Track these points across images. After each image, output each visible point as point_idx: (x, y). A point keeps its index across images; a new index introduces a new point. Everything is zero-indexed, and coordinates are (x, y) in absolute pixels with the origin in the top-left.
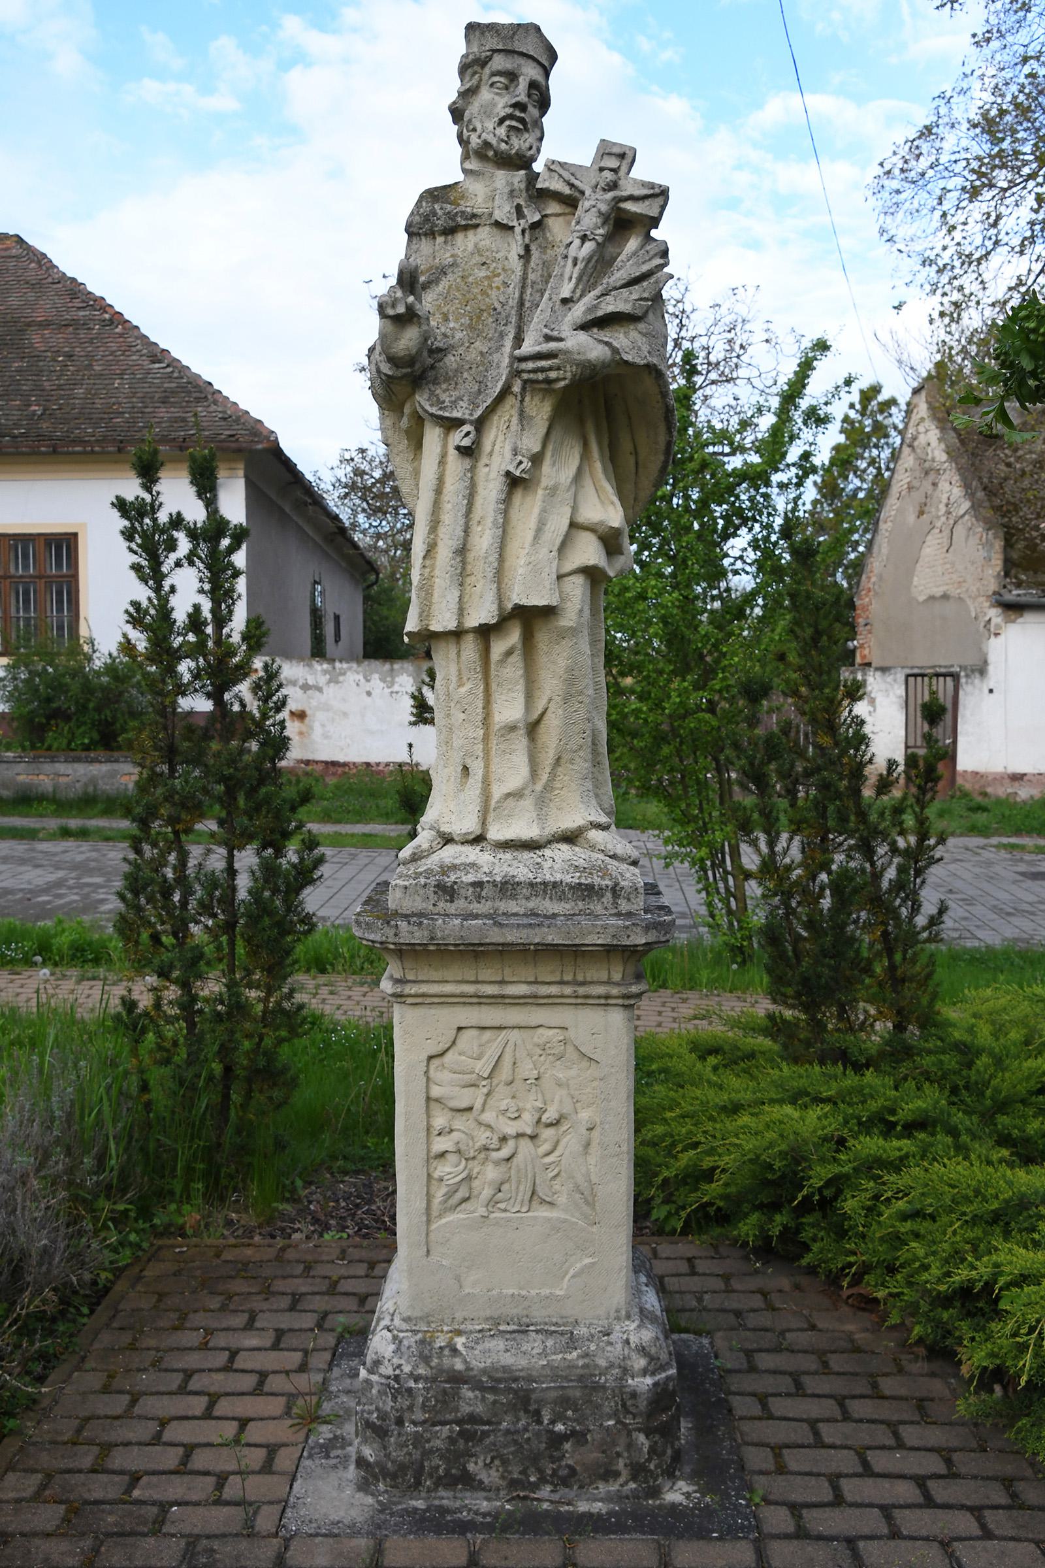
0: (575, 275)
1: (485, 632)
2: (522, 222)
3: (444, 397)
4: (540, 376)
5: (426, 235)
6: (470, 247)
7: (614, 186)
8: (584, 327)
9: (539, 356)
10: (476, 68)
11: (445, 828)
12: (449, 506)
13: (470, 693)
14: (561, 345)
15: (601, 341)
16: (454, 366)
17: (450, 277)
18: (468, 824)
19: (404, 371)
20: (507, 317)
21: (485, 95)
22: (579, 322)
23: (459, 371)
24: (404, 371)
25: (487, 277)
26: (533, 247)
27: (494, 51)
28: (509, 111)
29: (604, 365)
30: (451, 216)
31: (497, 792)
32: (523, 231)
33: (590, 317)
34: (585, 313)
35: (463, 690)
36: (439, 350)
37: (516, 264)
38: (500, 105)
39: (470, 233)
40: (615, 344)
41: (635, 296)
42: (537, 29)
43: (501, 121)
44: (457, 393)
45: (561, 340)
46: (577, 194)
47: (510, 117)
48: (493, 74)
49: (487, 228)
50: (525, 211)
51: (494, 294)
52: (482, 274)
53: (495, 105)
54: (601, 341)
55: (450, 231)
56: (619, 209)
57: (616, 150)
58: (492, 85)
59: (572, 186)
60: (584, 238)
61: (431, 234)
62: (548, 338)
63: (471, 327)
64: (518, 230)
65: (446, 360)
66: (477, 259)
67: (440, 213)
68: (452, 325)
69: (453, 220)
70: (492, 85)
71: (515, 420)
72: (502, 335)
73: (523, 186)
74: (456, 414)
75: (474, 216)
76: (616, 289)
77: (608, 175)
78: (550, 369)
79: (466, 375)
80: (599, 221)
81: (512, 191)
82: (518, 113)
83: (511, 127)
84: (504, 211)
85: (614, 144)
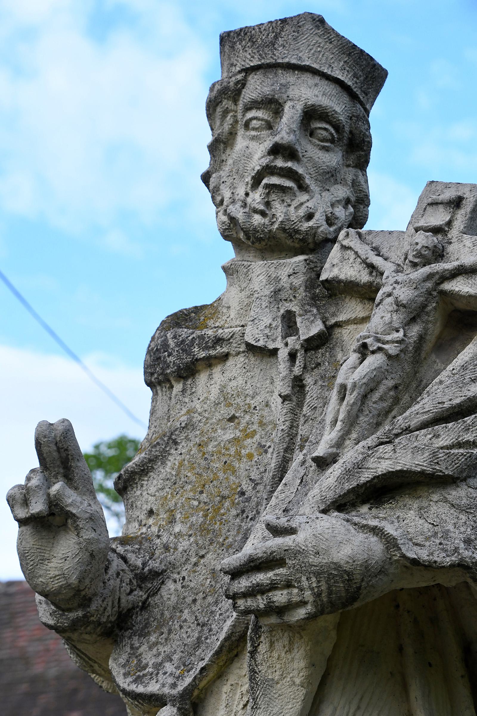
2: (291, 340)
4: (261, 602)
7: (438, 254)
8: (342, 504)
9: (254, 565)
10: (227, 104)
15: (364, 528)
16: (174, 599)
17: (183, 447)
19: (72, 615)
21: (241, 142)
22: (331, 496)
23: (177, 608)
24: (72, 615)
25: (236, 440)
26: (309, 380)
27: (248, 71)
28: (265, 161)
29: (370, 571)
30: (185, 346)
32: (292, 356)
33: (348, 486)
34: (340, 480)
36: (156, 574)
37: (278, 411)
38: (257, 156)
39: (217, 370)
40: (390, 529)
41: (444, 440)
42: (319, 22)
43: (257, 181)
44: (167, 649)
45: (292, 531)
47: (268, 170)
48: (247, 109)
49: (241, 359)
50: (299, 320)
51: (242, 466)
52: (229, 435)
54: (364, 528)
56: (443, 293)
57: (448, 195)
59: (371, 267)
60: (364, 350)
62: (276, 531)
63: (203, 529)
64: (283, 354)
65: (164, 592)
66: (225, 412)
67: (172, 343)
68: (177, 529)
73: (299, 281)
74: (153, 688)
75: (219, 341)
76: (408, 430)
77: (431, 240)
78: (273, 587)
79: (186, 614)
80: (397, 319)
81: (277, 292)
82: (280, 163)
83: (270, 187)
84: (261, 327)
85: (447, 186)
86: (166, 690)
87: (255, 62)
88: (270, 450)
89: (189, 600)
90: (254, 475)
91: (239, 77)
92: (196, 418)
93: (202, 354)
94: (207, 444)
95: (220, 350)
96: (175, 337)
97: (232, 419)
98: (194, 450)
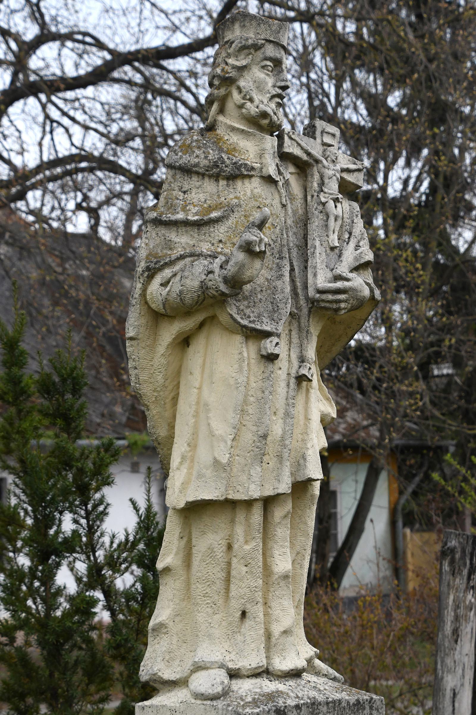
0: (337, 229)
1: (268, 502)
3: (248, 311)
5: (210, 177)
6: (249, 193)
10: (252, 51)
11: (231, 665)
12: (252, 399)
13: (254, 549)
14: (347, 284)
17: (236, 214)
18: (254, 659)
20: (280, 252)
31: (276, 629)
35: (247, 547)
39: (246, 181)
46: (311, 161)
48: (266, 59)
53: (266, 83)
55: (232, 178)
58: (263, 67)
59: (309, 154)
61: (216, 177)
64: (280, 184)
67: (228, 162)
69: (239, 169)
70: (263, 67)
71: (294, 334)
72: (279, 267)
75: (253, 169)
79: (259, 296)
86: (274, 330)
87: (272, 39)
88: (278, 228)
89: (259, 289)
90: (273, 237)
91: (263, 42)
92: (242, 203)
93: (246, 173)
94: (249, 217)
95: (252, 173)
96: (228, 158)
97: (259, 207)
98: (242, 218)
